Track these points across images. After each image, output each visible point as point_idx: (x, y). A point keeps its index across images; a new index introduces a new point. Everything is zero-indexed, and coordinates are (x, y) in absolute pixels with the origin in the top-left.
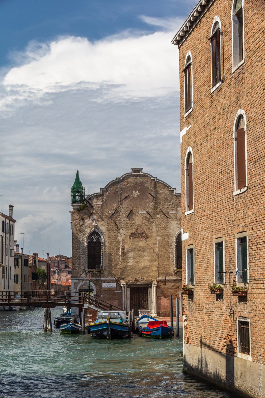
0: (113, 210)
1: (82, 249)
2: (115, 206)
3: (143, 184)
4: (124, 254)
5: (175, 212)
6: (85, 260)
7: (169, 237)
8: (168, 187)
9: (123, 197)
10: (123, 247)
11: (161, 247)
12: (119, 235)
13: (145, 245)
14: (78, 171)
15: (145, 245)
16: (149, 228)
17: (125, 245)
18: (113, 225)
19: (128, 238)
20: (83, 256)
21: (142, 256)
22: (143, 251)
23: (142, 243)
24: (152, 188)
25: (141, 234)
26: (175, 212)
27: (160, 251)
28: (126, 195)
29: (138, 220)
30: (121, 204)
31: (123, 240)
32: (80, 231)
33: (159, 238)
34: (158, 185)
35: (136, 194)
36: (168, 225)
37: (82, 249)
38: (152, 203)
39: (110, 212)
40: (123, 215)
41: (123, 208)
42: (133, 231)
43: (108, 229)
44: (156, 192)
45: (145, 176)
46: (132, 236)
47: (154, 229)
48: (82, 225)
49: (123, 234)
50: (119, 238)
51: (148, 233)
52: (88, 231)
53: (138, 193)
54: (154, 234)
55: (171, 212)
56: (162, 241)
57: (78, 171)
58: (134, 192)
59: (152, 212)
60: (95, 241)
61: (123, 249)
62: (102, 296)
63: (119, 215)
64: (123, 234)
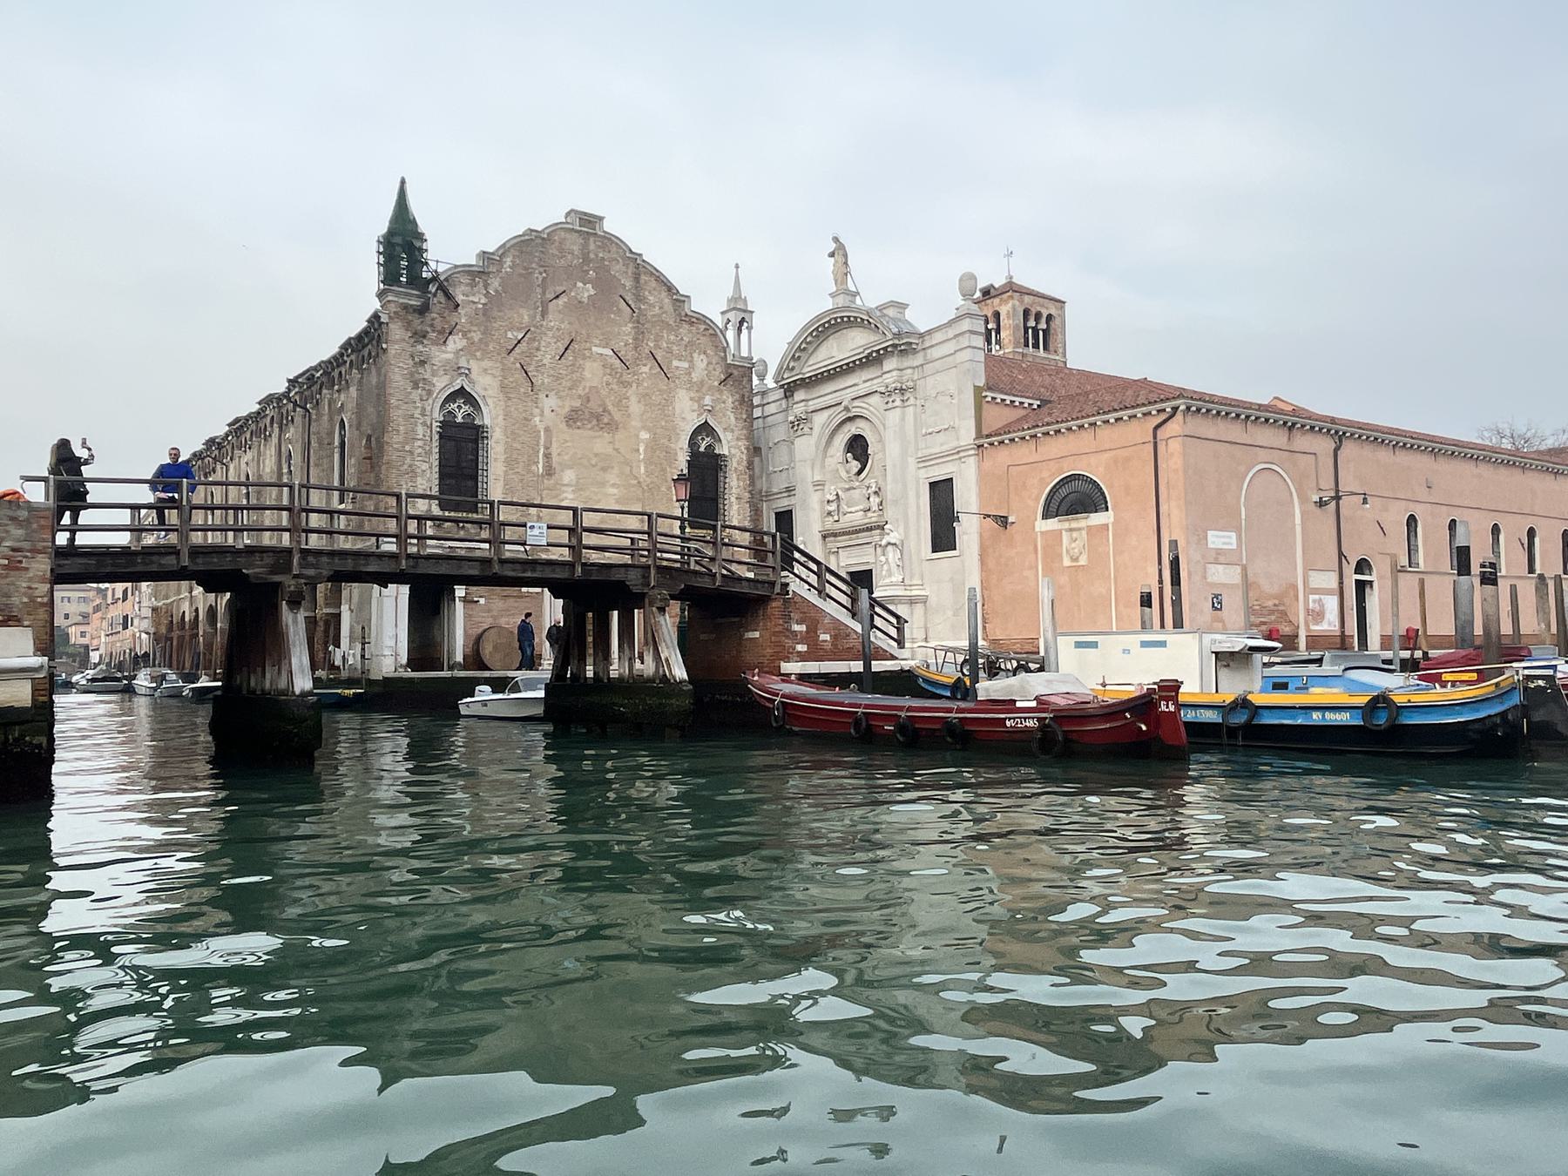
0: (519, 329)
1: (420, 443)
2: (526, 316)
3: (602, 269)
4: (549, 471)
5: (686, 365)
6: (429, 480)
7: (672, 432)
8: (670, 289)
9: (550, 296)
10: (547, 448)
11: (649, 461)
12: (537, 411)
13: (609, 450)
14: (403, 182)
15: (609, 450)
16: (621, 403)
17: (554, 445)
18: (521, 376)
19: (563, 426)
20: (425, 466)
21: (603, 484)
22: (604, 469)
23: (601, 444)
24: (629, 283)
25: (598, 418)
26: (686, 365)
27: (649, 473)
28: (560, 289)
29: (592, 374)
30: (544, 314)
31: (547, 430)
32: (416, 387)
33: (645, 435)
34: (643, 278)
35: (586, 291)
36: (669, 401)
37: (420, 443)
38: (629, 328)
39: (510, 335)
40: (548, 352)
41: (551, 329)
42: (577, 404)
43: (503, 387)
44: (639, 298)
45: (610, 241)
46: (573, 419)
47: (635, 407)
48: (423, 363)
49: (551, 407)
50: (537, 419)
51: (617, 416)
52: (443, 385)
53: (590, 290)
54: (636, 423)
55: (675, 363)
56: (653, 446)
57: (403, 182)
58: (580, 284)
59: (629, 355)
60: (459, 419)
61: (547, 456)
62: (482, 601)
63: (538, 349)
64: (547, 412)
